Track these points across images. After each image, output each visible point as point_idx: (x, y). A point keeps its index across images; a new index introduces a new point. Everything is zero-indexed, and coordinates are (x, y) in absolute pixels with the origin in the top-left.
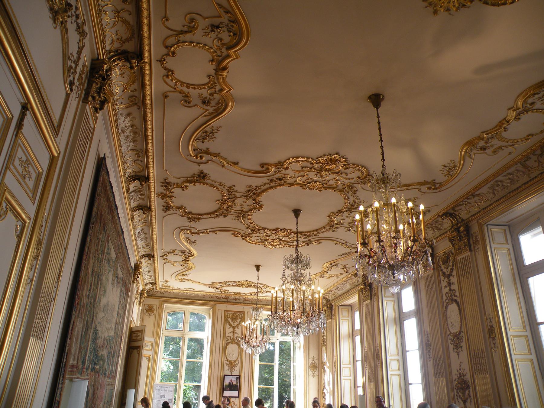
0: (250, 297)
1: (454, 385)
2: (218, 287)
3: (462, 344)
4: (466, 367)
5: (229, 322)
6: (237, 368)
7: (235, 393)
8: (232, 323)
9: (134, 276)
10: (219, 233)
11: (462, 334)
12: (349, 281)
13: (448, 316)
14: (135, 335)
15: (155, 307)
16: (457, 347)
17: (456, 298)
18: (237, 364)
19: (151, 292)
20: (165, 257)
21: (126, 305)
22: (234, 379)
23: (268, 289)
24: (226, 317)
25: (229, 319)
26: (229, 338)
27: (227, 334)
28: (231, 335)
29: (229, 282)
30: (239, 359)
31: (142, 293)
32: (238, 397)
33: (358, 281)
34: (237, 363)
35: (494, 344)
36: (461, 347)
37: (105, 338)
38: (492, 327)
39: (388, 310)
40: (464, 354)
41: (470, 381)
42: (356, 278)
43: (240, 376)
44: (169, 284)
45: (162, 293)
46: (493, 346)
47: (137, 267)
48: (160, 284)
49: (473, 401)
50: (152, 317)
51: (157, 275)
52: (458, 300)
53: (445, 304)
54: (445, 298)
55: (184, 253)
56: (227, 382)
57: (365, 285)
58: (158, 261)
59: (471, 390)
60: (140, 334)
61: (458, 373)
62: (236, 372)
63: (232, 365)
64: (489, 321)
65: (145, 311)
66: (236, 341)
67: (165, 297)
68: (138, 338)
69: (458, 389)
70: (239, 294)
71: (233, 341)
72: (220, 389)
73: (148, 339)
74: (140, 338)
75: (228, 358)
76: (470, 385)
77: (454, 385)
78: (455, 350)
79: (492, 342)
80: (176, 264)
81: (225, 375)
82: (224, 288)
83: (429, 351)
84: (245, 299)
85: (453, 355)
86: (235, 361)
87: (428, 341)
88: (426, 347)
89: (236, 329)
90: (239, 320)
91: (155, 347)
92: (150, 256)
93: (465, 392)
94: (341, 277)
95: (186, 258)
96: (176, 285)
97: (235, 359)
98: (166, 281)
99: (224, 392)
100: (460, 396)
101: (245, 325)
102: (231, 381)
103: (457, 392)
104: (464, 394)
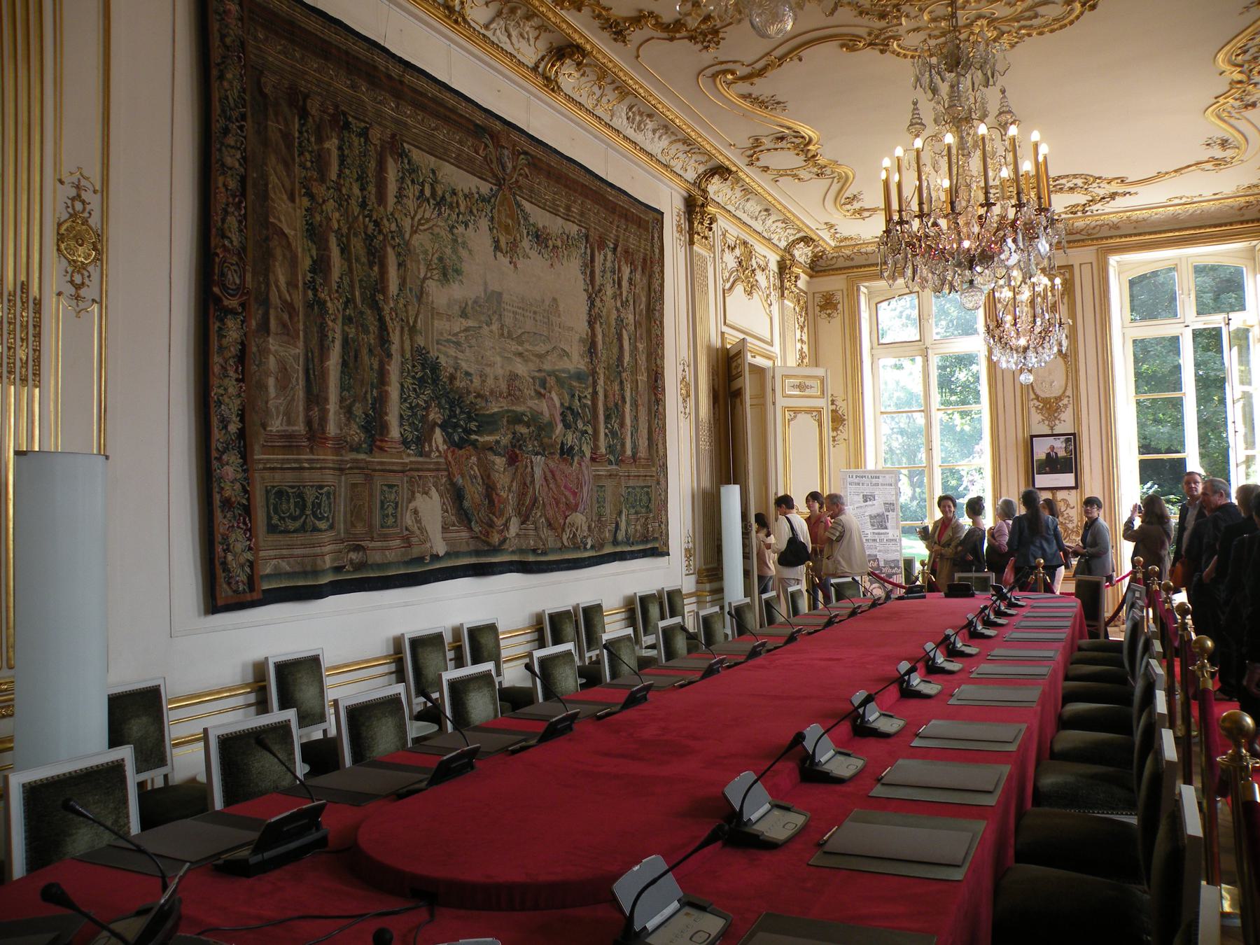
6: (1067, 415)
7: (1067, 479)
15: (839, 297)
18: (1066, 406)
19: (821, 262)
22: (1059, 444)
23: (1114, 187)
30: (1069, 393)
32: (1076, 487)
34: (1065, 401)
43: (1074, 434)
45: (849, 258)
50: (837, 321)
56: (1041, 452)
62: (1065, 427)
67: (857, 267)
72: (1027, 472)
75: (1039, 392)
81: (1032, 437)
86: (1059, 399)
97: (1057, 393)
99: (1036, 476)
102: (1052, 448)
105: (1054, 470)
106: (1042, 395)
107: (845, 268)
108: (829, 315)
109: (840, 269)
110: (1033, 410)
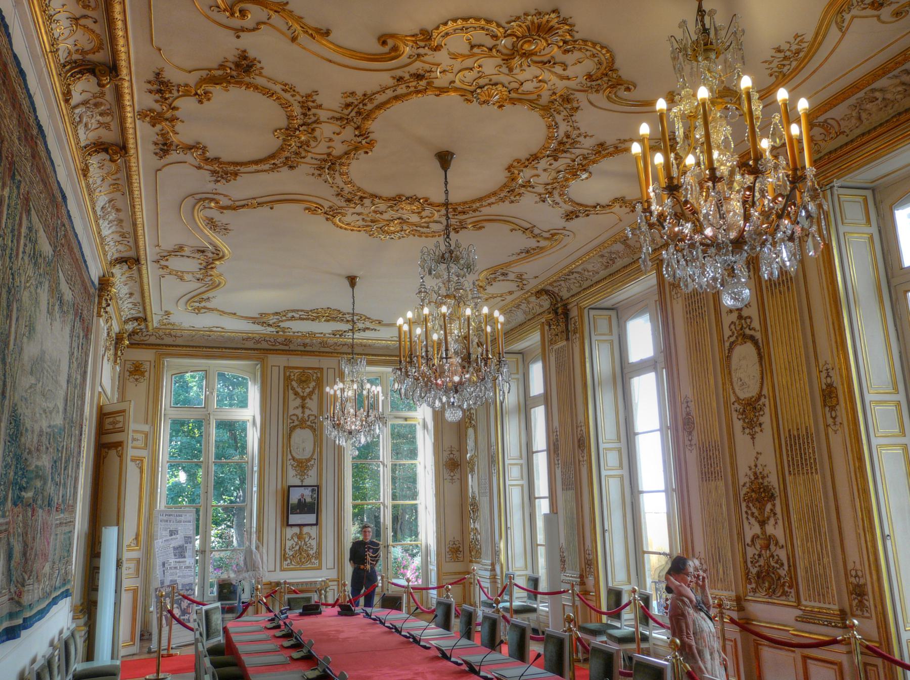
0: (331, 341)
2: (271, 322)
3: (761, 419)
4: (769, 462)
5: (293, 389)
6: (313, 473)
8: (299, 390)
9: (100, 303)
10: (277, 206)
11: (763, 399)
12: (524, 306)
13: (733, 367)
14: (111, 420)
15: (146, 366)
16: (752, 425)
17: (752, 333)
20: (163, 263)
21: (86, 361)
24: (288, 379)
25: (294, 383)
26: (294, 418)
27: (291, 412)
28: (299, 412)
29: (293, 311)
30: (315, 456)
31: (119, 339)
33: (541, 306)
34: (312, 462)
35: (834, 418)
36: (760, 425)
37: (41, 431)
38: (830, 386)
39: (601, 361)
40: (765, 439)
41: (776, 486)
42: (538, 301)
44: (173, 319)
46: (830, 421)
47: (104, 284)
48: (155, 321)
49: (780, 522)
50: (143, 385)
51: (147, 301)
52: (758, 335)
53: (727, 344)
54: (727, 333)
55: (203, 252)
57: (556, 313)
58: (150, 271)
59: (778, 502)
60: (120, 419)
62: (311, 480)
63: (302, 466)
64: (824, 374)
65: (127, 374)
66: (309, 423)
68: (117, 426)
69: (748, 500)
70: (312, 335)
71: (303, 424)
73: (135, 426)
74: (120, 425)
75: (294, 455)
76: (777, 493)
77: (742, 493)
78: (747, 431)
79: (828, 415)
80: (187, 277)
82: (282, 325)
83: (690, 433)
84: (323, 344)
85: (742, 439)
86: (309, 460)
87: (688, 414)
88: (681, 426)
89: (308, 400)
90: (312, 384)
91: (151, 441)
92: (132, 261)
93: (765, 505)
94: (509, 298)
95: (208, 264)
96: (187, 320)
98: (167, 313)
100: (753, 514)
101: (332, 392)
103: (748, 507)
106: (297, 457)
108: (137, 380)
109: (152, 345)
110: (290, 467)
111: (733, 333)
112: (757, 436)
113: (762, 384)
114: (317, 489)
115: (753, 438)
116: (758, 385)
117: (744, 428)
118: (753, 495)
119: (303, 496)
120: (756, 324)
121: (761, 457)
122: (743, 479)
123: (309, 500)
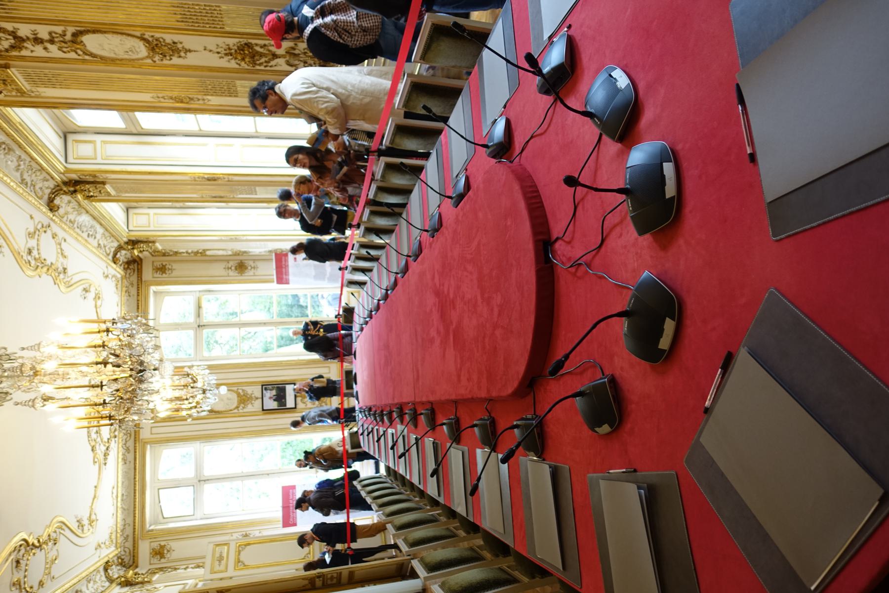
1: (247, 67)
3: (168, 41)
4: (212, 42)
6: (249, 390)
11: (146, 37)
13: (113, 55)
15: (155, 545)
16: (175, 49)
19: (126, 560)
30: (235, 389)
34: (240, 391)
36: (174, 43)
40: (187, 41)
41: (237, 40)
45: (126, 538)
50: (173, 545)
52: (71, 30)
53: (87, 57)
59: (254, 42)
61: (227, 58)
62: (257, 391)
63: (244, 399)
65: (163, 560)
69: (254, 64)
76: (245, 41)
77: (247, 67)
78: (182, 54)
85: (191, 60)
86: (239, 395)
87: (171, 98)
93: (257, 52)
100: (266, 62)
103: (260, 64)
104: (262, 55)
105: (284, 397)
106: (235, 405)
107: (134, 541)
108: (168, 551)
109: (134, 544)
110: (245, 410)
111: (72, 51)
112: (187, 47)
113: (129, 35)
114: (265, 386)
115: (190, 51)
116: (129, 38)
117: (180, 57)
118: (247, 60)
119: (270, 398)
120: (59, 29)
121: (209, 47)
122: (233, 64)
123: (274, 392)
